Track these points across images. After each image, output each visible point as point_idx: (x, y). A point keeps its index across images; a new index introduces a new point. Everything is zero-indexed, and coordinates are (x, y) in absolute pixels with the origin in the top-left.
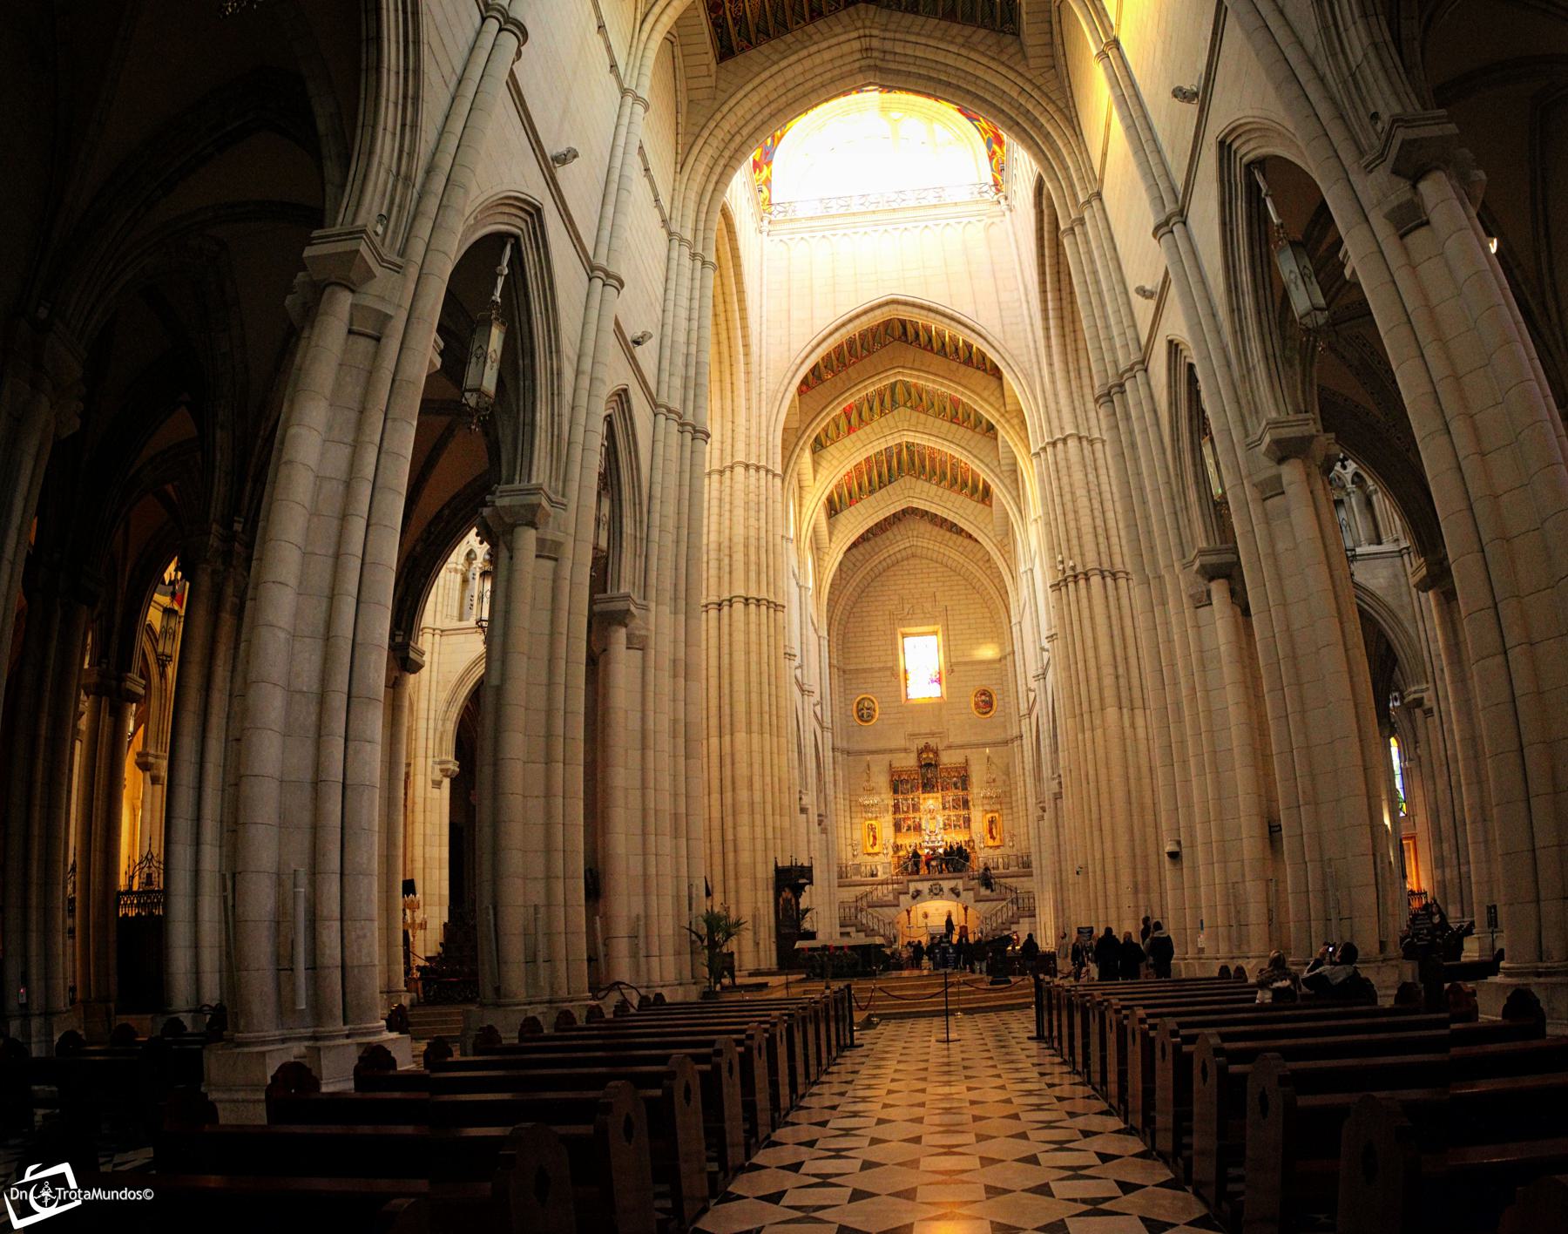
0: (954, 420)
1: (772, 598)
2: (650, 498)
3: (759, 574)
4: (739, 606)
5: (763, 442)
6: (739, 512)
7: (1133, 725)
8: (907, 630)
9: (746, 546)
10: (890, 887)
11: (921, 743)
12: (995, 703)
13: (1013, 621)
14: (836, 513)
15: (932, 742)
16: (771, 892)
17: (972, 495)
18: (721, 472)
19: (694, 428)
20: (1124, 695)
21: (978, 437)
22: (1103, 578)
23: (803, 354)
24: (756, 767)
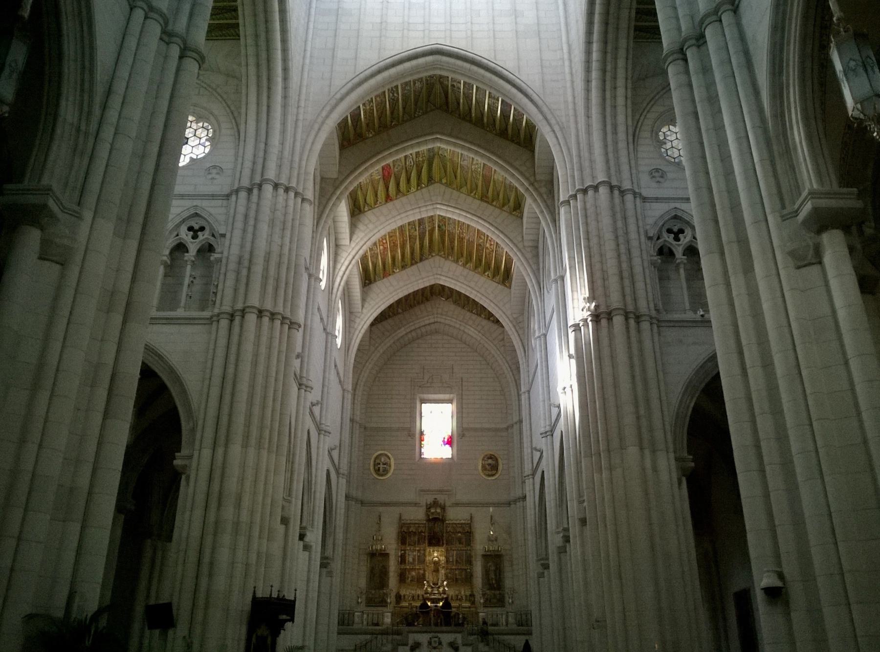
0: (483, 198)
1: (288, 314)
2: (109, 92)
3: (276, 289)
4: (252, 318)
5: (296, 165)
6: (264, 228)
7: (655, 469)
8: (426, 396)
9: (267, 260)
10: (390, 637)
11: (430, 499)
12: (500, 467)
13: (523, 389)
14: (370, 283)
15: (441, 498)
16: (244, 630)
17: (494, 276)
18: (250, 191)
19: (185, 42)
20: (646, 436)
21: (505, 214)
22: (627, 319)
23: (344, 91)
24: (248, 484)
